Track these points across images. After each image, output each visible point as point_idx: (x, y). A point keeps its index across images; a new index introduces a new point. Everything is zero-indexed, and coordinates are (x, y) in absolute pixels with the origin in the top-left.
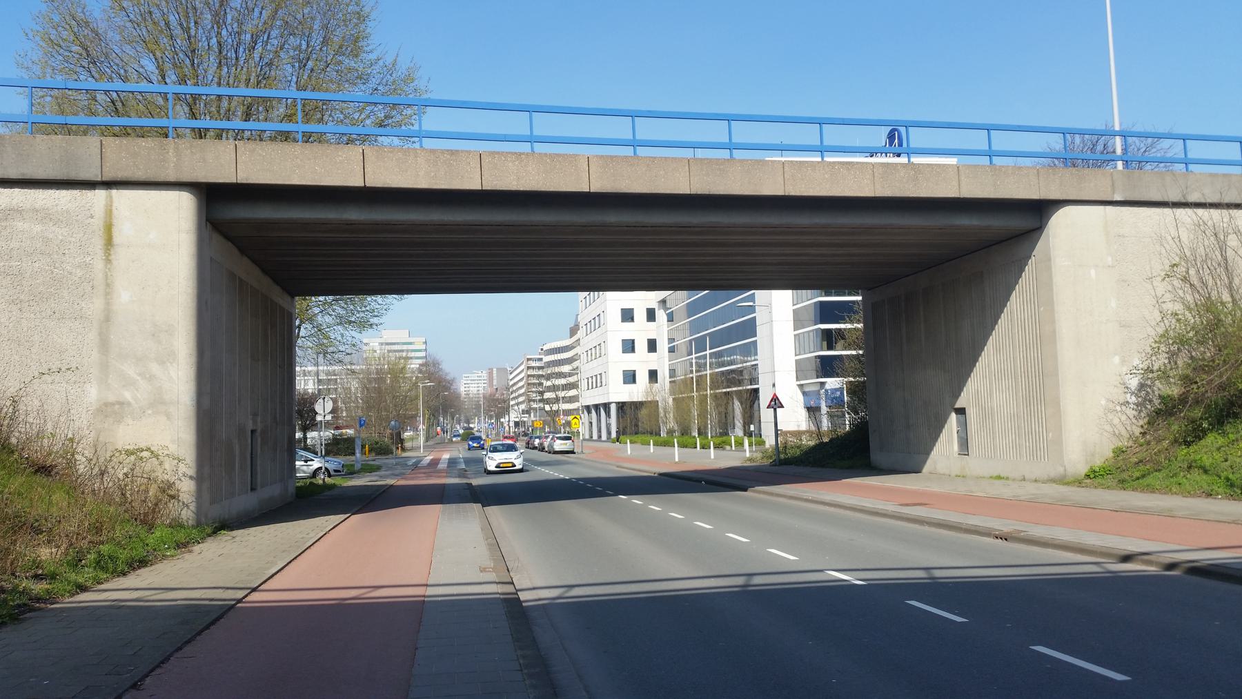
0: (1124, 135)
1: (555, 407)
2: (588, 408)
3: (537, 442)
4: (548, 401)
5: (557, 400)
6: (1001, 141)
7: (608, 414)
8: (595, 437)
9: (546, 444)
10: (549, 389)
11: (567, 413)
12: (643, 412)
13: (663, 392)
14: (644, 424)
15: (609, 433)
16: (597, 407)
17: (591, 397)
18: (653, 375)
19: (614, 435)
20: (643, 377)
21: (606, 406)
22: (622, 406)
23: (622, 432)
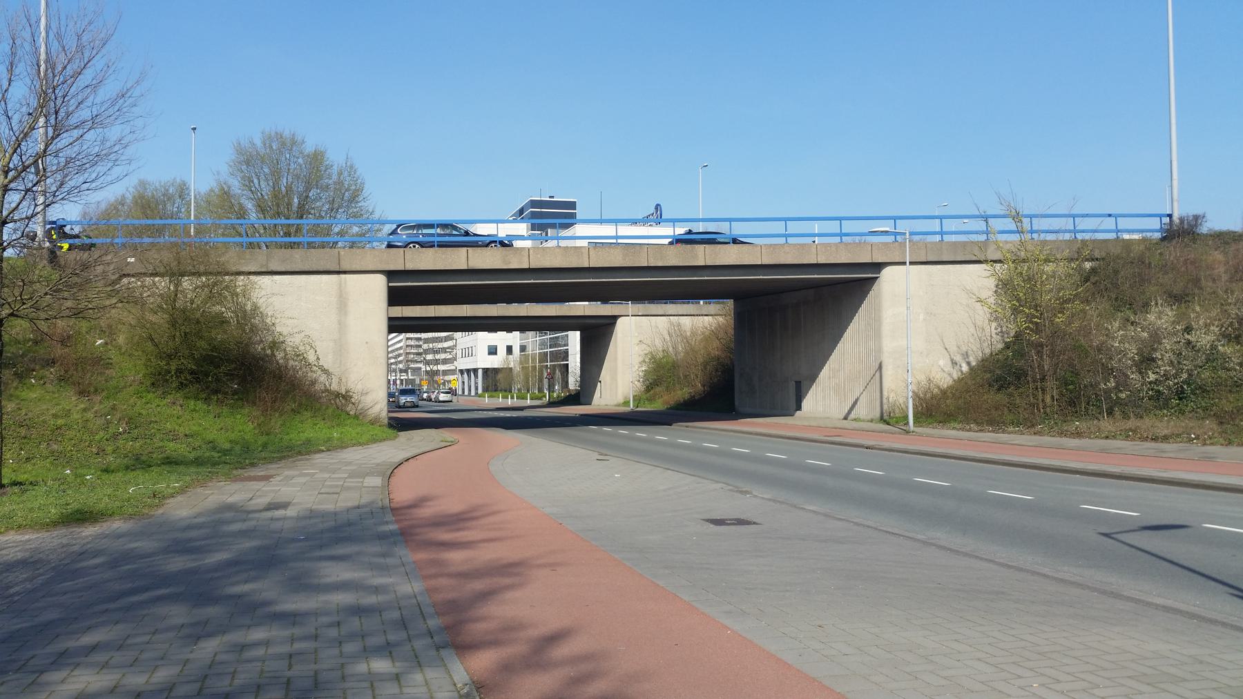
0: (1031, 217)
1: (435, 368)
2: (462, 372)
3: (425, 395)
4: (428, 363)
5: (437, 362)
6: (848, 227)
7: (476, 376)
8: (466, 393)
9: (433, 397)
10: (426, 352)
11: (445, 373)
12: (500, 376)
13: (514, 361)
14: (502, 385)
15: (477, 388)
16: (468, 371)
17: (463, 364)
18: (509, 350)
19: (480, 391)
20: (502, 351)
21: (475, 371)
22: (486, 371)
23: (486, 389)
